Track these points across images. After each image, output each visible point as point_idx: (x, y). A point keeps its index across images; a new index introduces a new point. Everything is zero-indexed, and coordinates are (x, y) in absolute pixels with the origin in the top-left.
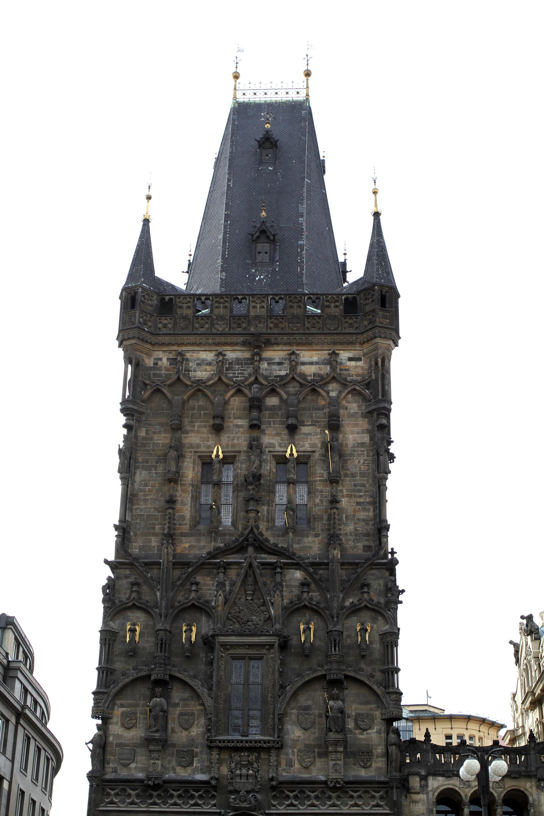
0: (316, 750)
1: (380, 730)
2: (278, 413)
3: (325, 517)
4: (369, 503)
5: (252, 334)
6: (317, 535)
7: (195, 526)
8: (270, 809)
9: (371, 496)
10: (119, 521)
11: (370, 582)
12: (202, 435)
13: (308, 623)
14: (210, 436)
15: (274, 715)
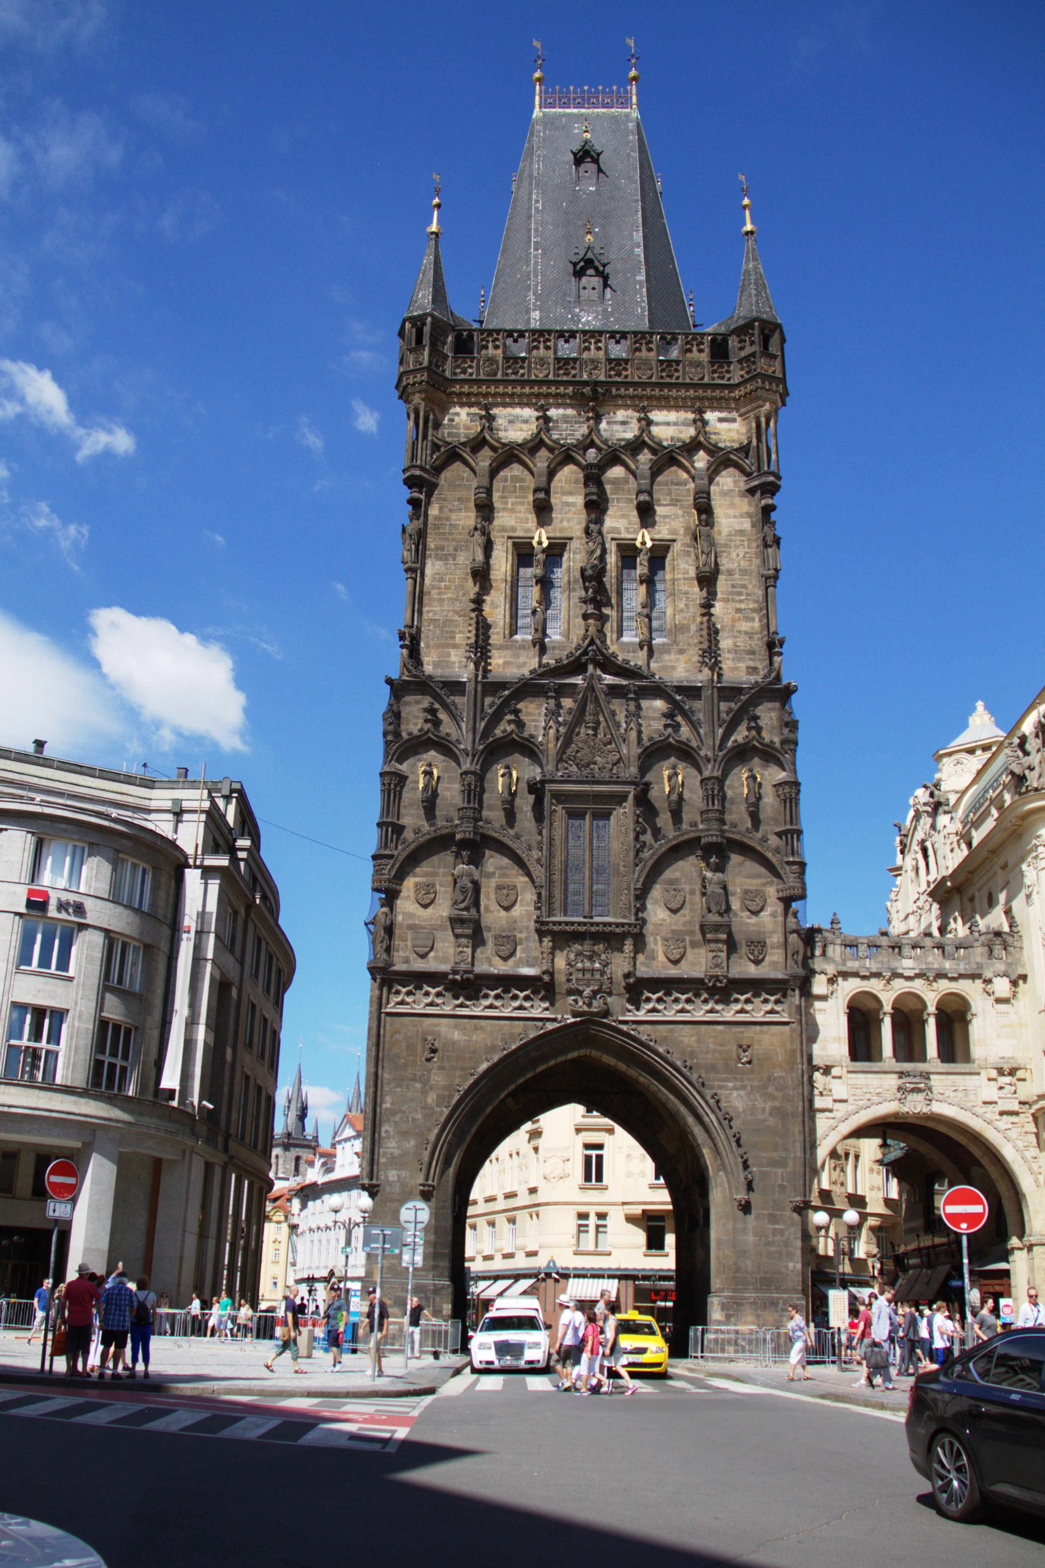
0: (688, 938)
1: (775, 912)
2: (623, 490)
3: (693, 628)
4: (753, 610)
5: (586, 383)
6: (681, 652)
7: (511, 635)
8: (624, 1015)
9: (755, 601)
11: (758, 714)
12: (518, 515)
13: (674, 767)
14: (530, 516)
15: (628, 889)
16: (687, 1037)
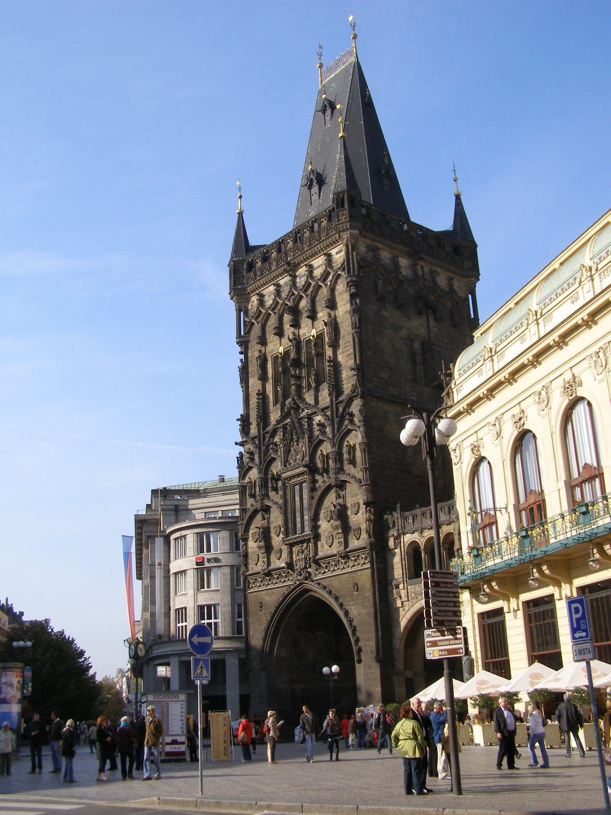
1: (363, 512)
7: (276, 404)
10: (242, 415)
14: (277, 341)
16: (335, 584)
